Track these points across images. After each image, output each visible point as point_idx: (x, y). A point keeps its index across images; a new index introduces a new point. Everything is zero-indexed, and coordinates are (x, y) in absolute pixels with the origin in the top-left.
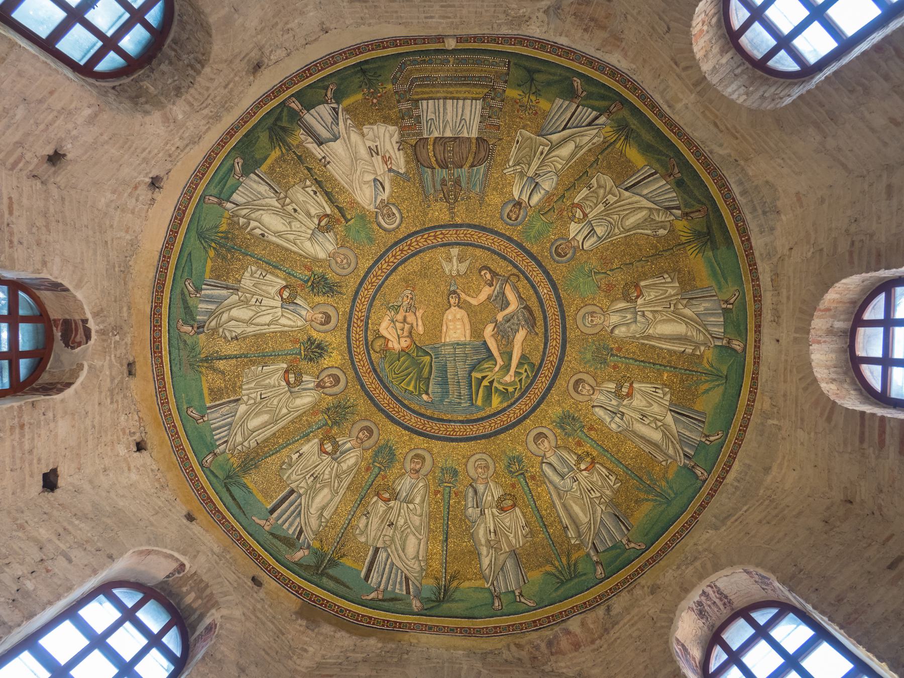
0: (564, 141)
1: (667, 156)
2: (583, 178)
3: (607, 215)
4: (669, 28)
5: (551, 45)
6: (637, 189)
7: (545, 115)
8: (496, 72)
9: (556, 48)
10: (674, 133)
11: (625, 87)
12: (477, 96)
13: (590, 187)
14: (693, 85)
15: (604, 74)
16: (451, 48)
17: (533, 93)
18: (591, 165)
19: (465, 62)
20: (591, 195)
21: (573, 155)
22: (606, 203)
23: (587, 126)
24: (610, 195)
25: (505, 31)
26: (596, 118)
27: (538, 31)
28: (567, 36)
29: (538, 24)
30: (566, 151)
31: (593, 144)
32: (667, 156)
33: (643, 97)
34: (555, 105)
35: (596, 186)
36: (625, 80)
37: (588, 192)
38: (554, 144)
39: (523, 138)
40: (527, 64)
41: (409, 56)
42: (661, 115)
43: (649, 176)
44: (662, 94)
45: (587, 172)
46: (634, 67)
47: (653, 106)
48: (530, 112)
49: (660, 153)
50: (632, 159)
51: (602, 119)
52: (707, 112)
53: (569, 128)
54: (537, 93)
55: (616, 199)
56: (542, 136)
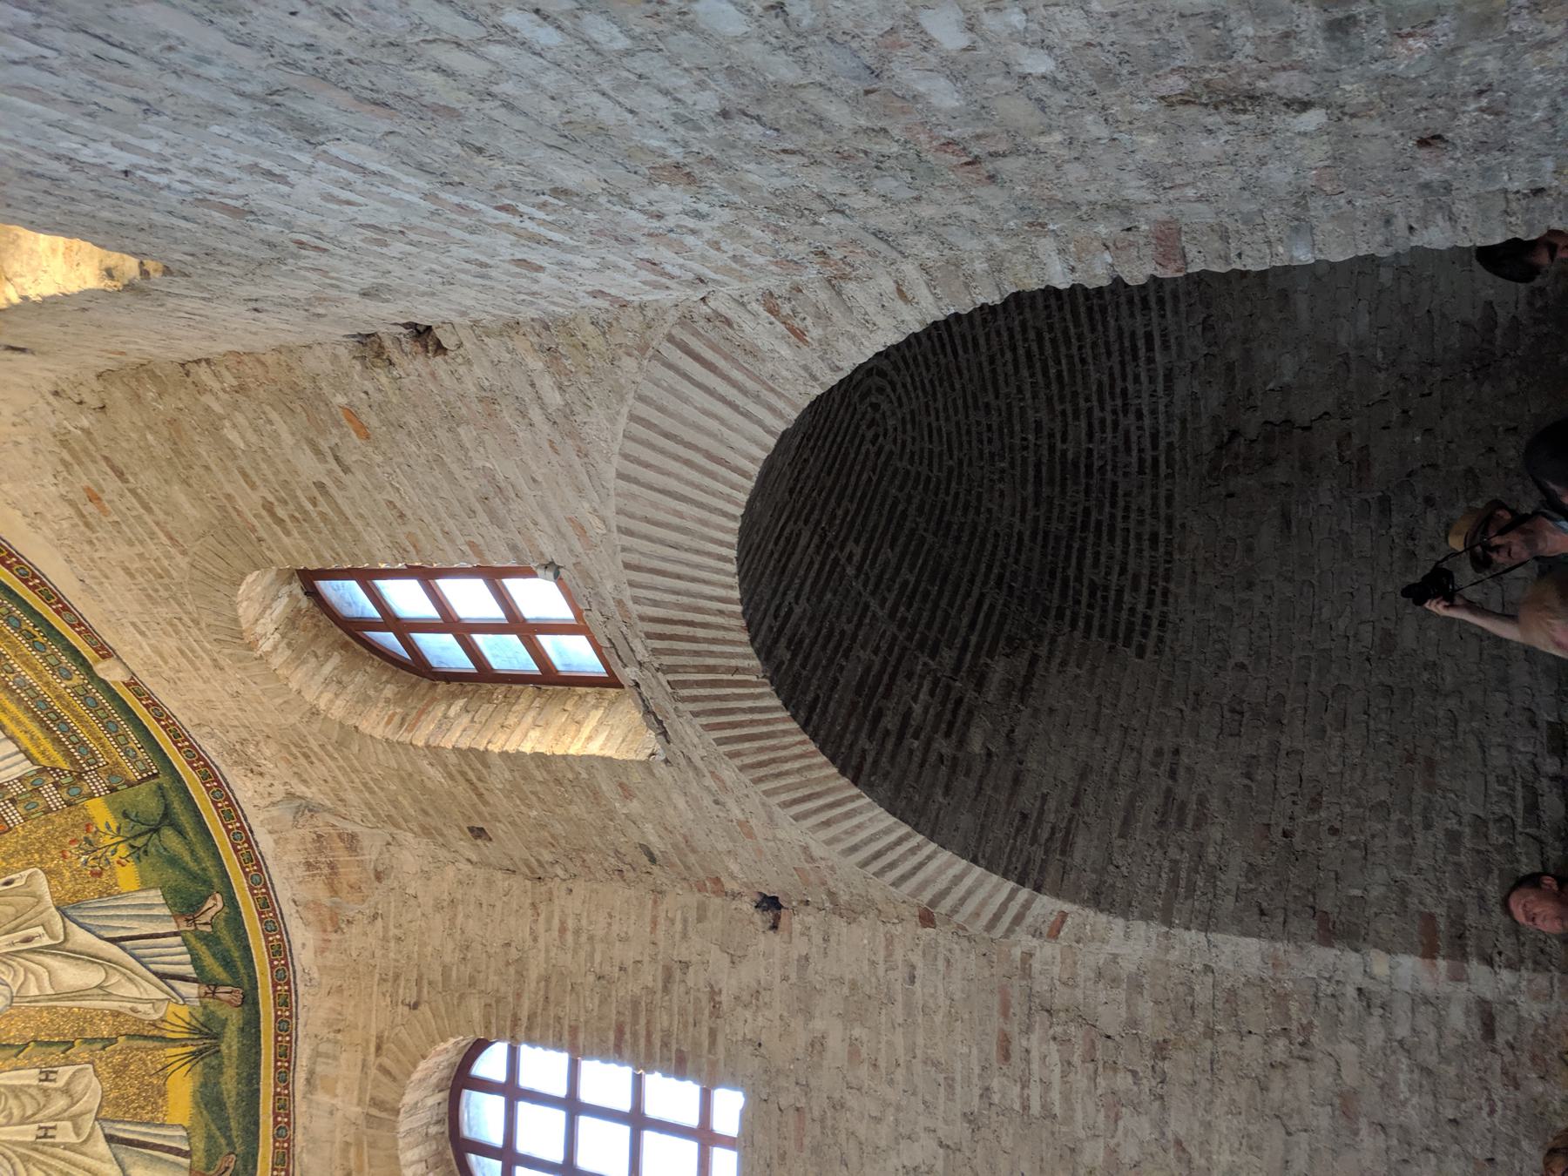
0: (94, 958)
1: (230, 1143)
2: (53, 1049)
3: (25, 1159)
4: (415, 1006)
5: (242, 827)
6: (125, 1154)
7: (106, 892)
8: (117, 764)
9: (243, 836)
10: (276, 1123)
11: (275, 985)
12: (38, 756)
13: (47, 1076)
14: (372, 1099)
15: (266, 937)
16: (101, 675)
17: (132, 847)
18: (86, 1041)
19: (94, 707)
20: (34, 1092)
21: (80, 994)
22: (45, 1133)
23: (156, 973)
24: (69, 1124)
25: (209, 748)
26: (183, 978)
27: (250, 794)
28: (276, 842)
29: (260, 789)
30: (73, 976)
31: (133, 1010)
32: (230, 1143)
33: (284, 1026)
34: (144, 894)
35: (61, 1083)
36: (283, 975)
37: (35, 1082)
38: (69, 946)
39: (26, 885)
40: (177, 806)
41: (18, 607)
42: (283, 1076)
43: (170, 1150)
44: (317, 1054)
45: (71, 1045)
46: (316, 976)
47: (285, 1054)
48: (92, 863)
49: (225, 1130)
50: (170, 1095)
51: (191, 990)
52: (353, 1150)
53: (123, 948)
54: (139, 853)
55: (73, 1139)
56: (64, 914)
